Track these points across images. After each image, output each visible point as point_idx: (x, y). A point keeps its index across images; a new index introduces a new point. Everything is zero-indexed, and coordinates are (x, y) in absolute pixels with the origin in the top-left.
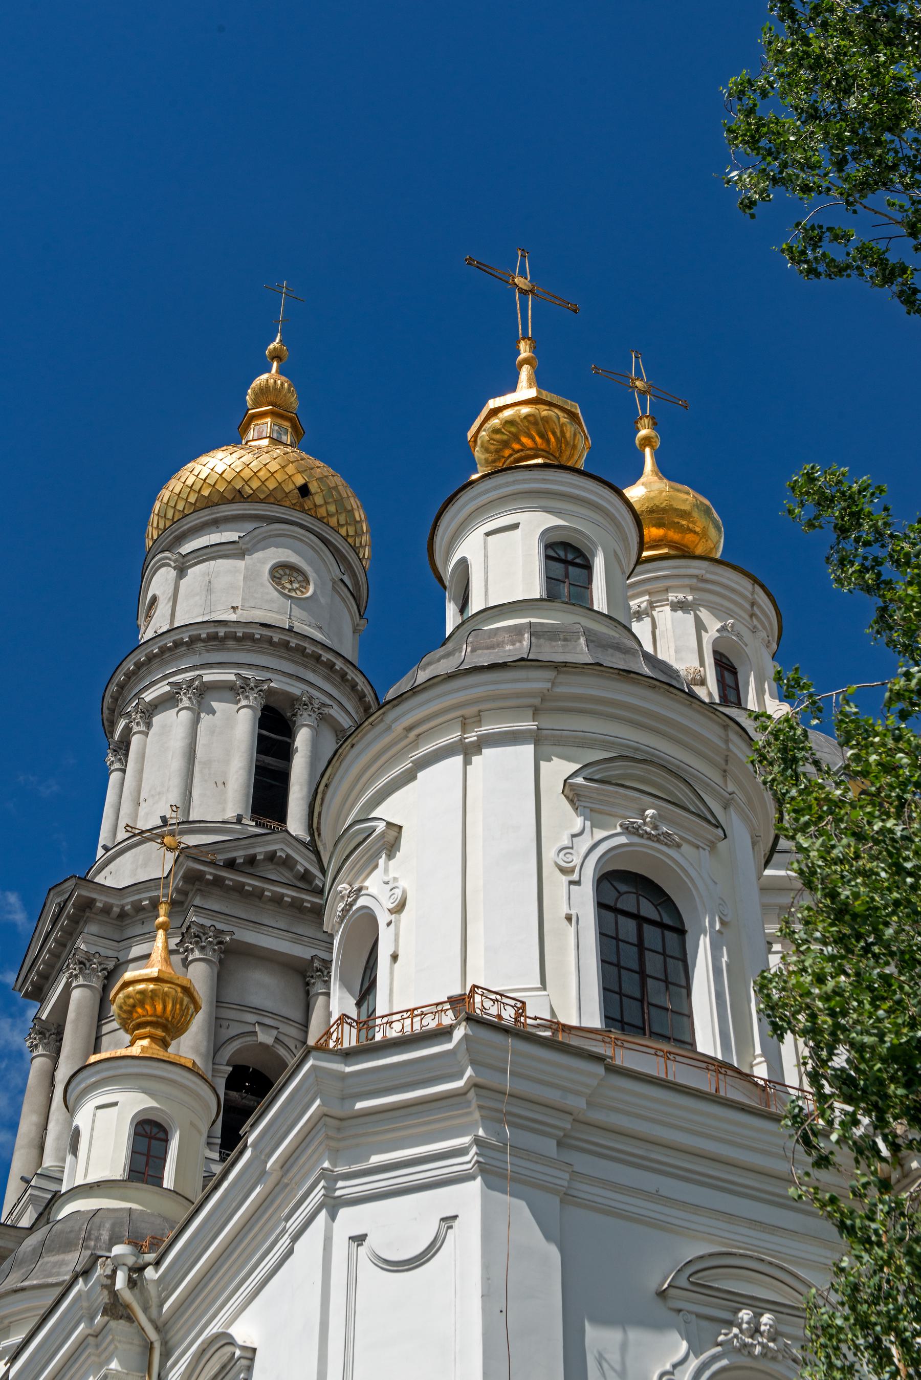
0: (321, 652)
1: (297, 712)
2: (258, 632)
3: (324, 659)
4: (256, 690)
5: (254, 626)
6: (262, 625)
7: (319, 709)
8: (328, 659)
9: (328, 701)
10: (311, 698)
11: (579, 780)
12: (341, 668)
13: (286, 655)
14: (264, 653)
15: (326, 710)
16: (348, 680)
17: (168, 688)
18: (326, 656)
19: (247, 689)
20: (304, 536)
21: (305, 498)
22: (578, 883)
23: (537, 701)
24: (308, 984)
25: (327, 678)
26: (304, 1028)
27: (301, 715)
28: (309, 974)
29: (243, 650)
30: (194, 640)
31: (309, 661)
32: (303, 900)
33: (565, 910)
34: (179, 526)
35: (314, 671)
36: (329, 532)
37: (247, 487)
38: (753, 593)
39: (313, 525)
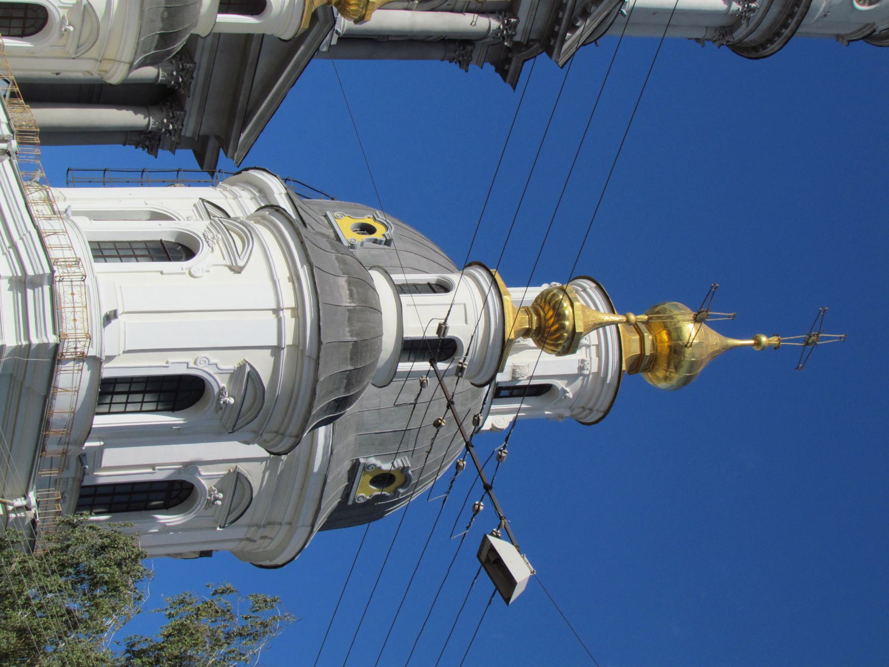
0: (796, 19)
3: (790, 21)
7: (745, 16)
8: (790, 24)
9: (752, 25)
11: (248, 369)
12: (783, 34)
15: (744, 22)
16: (774, 37)
18: (793, 23)
22: (188, 368)
23: (301, 348)
24: (500, 13)
26: (464, 10)
28: (508, 13)
32: (564, 12)
33: (171, 361)
35: (780, 12)
38: (597, 410)
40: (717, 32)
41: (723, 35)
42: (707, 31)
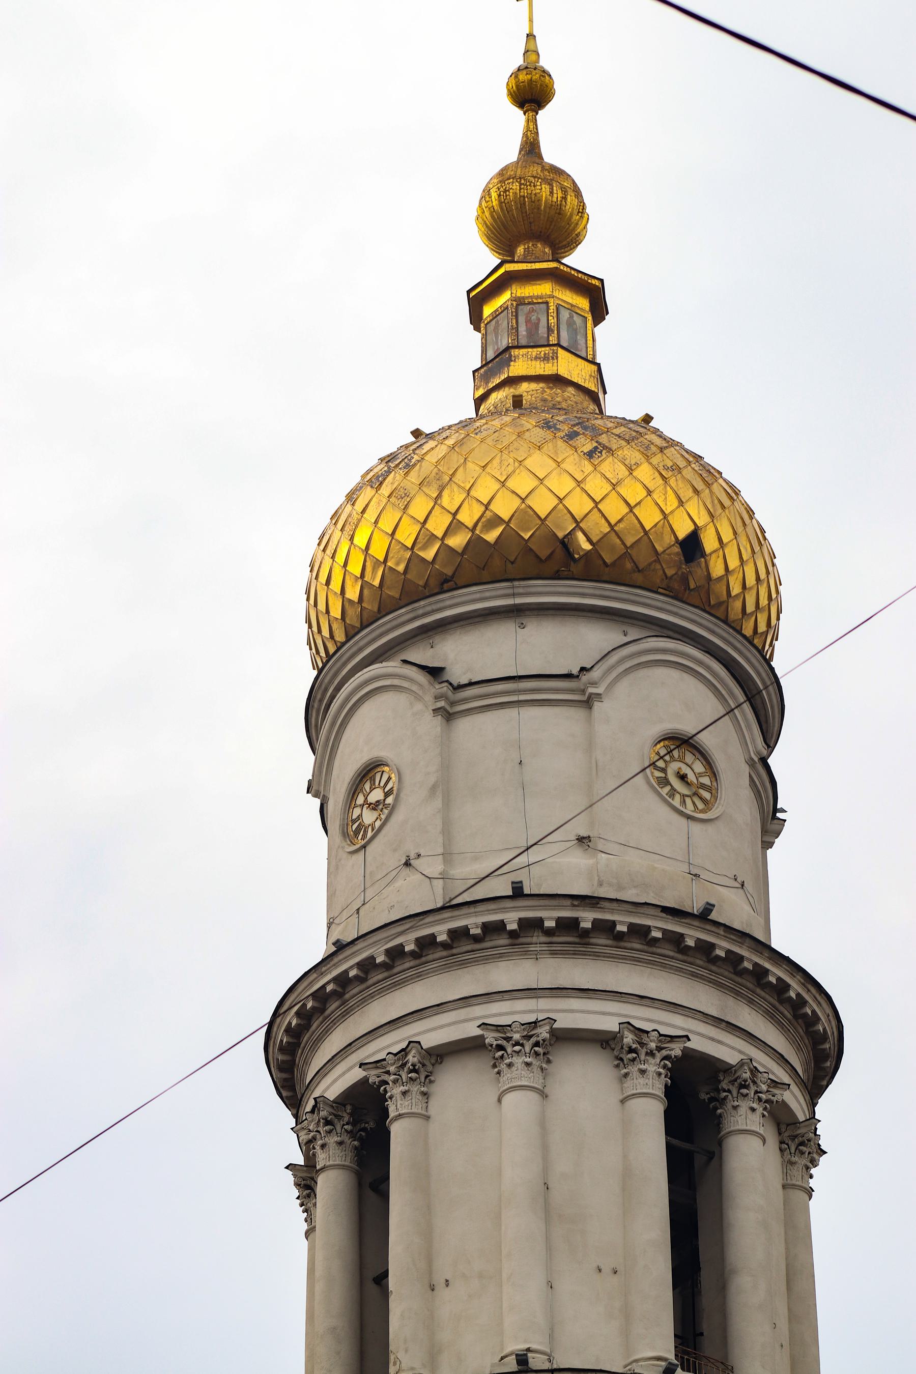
0: (767, 965)
1: (726, 1098)
2: (658, 925)
4: (659, 1056)
5: (652, 911)
6: (666, 910)
8: (779, 979)
10: (754, 1071)
13: (704, 972)
14: (663, 966)
17: (472, 1030)
19: (643, 1052)
20: (700, 663)
21: (692, 564)
25: (771, 1015)
27: (735, 1108)
29: (624, 958)
30: (530, 925)
31: (744, 982)
34: (434, 607)
36: (739, 645)
37: (580, 537)
39: (713, 632)
40: (793, 1159)
41: (802, 1144)
42: (794, 1186)
